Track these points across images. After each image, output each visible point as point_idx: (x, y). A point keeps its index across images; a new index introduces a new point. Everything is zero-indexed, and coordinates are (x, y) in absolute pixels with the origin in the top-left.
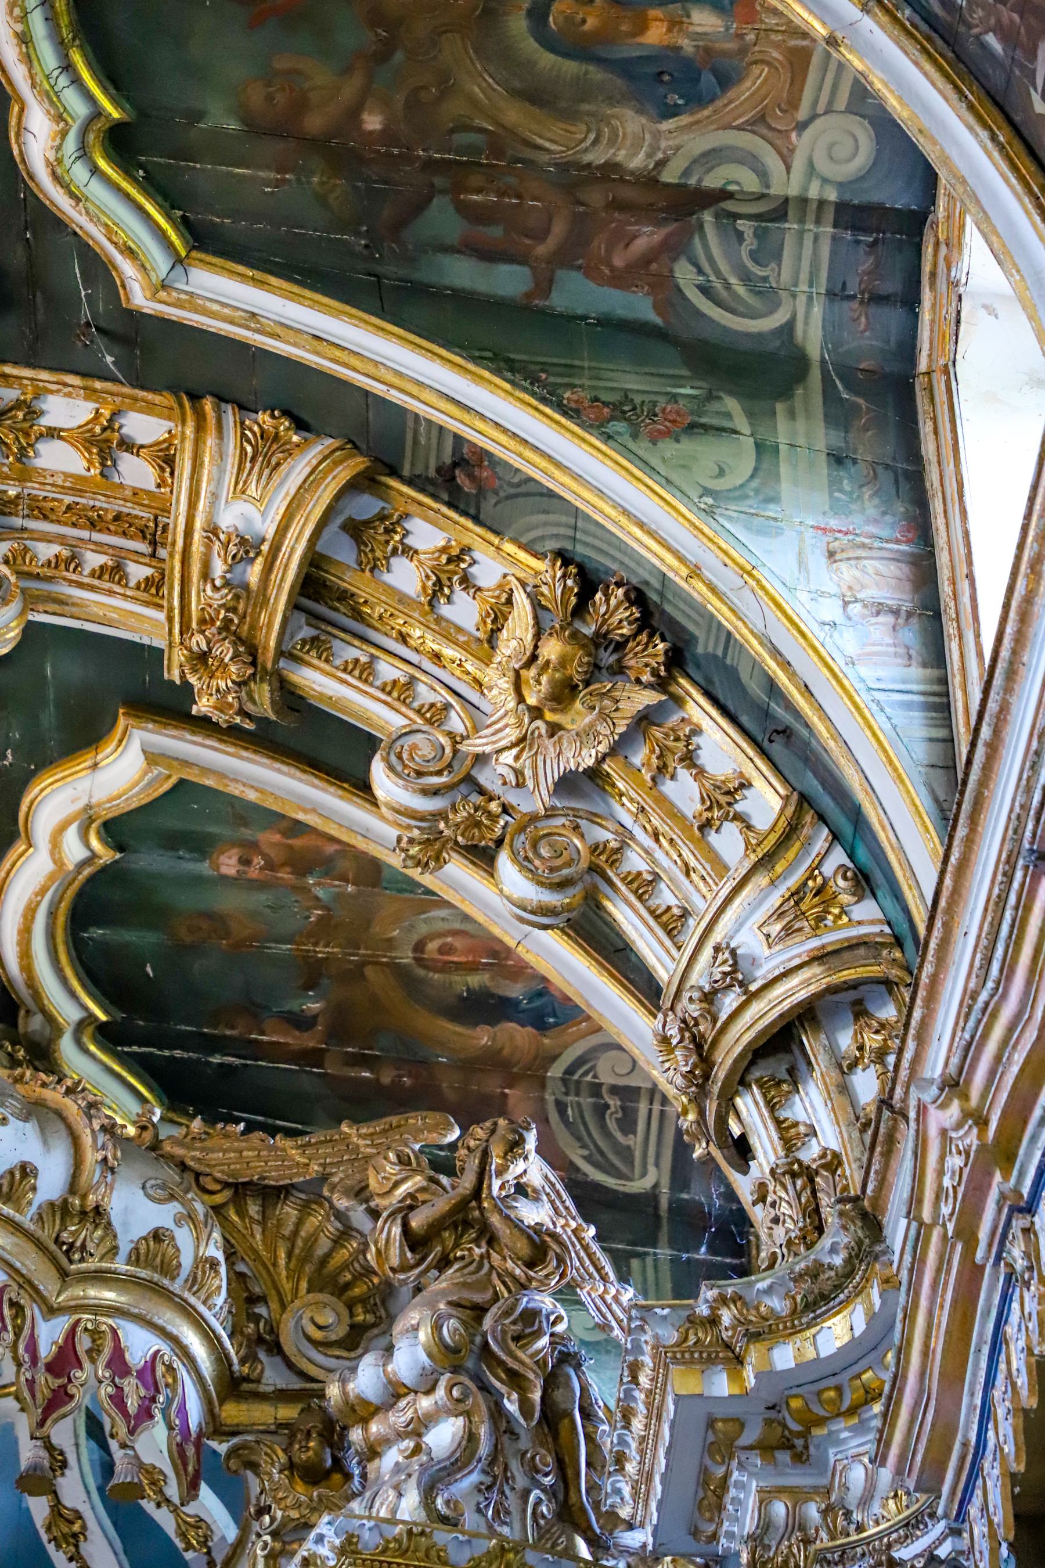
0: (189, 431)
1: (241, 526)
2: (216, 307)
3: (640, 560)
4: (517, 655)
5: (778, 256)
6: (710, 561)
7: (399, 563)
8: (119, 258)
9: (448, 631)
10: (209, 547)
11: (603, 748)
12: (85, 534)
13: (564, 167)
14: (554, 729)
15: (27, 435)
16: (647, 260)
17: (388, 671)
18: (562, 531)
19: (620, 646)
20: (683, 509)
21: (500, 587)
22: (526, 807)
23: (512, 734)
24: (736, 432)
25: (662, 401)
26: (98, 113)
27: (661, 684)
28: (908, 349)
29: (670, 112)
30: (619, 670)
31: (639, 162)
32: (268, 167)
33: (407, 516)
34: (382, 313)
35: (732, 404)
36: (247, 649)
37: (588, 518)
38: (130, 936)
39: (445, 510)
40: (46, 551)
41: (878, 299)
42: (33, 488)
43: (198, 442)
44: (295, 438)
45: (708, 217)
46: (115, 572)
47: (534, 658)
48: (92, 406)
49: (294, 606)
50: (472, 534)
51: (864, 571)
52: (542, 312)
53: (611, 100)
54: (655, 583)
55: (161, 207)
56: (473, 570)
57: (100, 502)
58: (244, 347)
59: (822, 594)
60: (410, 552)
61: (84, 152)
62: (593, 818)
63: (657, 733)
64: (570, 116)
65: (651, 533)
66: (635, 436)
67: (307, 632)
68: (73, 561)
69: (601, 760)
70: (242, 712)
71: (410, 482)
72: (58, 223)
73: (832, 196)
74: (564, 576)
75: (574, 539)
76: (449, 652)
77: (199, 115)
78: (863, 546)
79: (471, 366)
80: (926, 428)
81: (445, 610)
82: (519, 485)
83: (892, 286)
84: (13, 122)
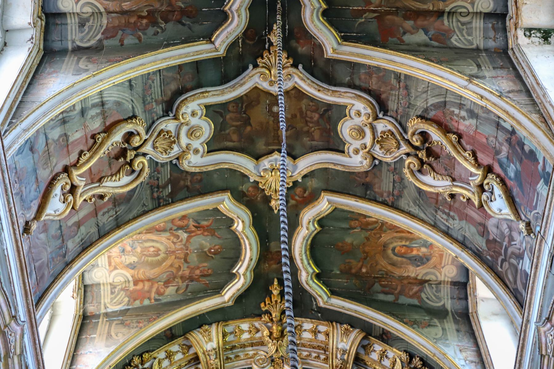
0: (331, 329)
1: (342, 347)
2: (336, 306)
6: (437, 352)
8: (318, 297)
12: (312, 350)
15: (301, 331)
18: (405, 346)
20: (430, 342)
24: (437, 326)
26: (314, 271)
32: (345, 279)
39: (381, 342)
40: (305, 353)
42: (302, 341)
44: (351, 329)
46: (318, 357)
48: (312, 325)
51: (467, 354)
55: (325, 288)
56: (388, 354)
57: (315, 343)
58: (340, 313)
59: (461, 359)
61: (312, 279)
65: (425, 347)
68: (310, 355)
74: (406, 355)
75: (407, 348)
77: (332, 271)
78: (466, 349)
79: (386, 315)
82: (396, 337)
84: (299, 274)
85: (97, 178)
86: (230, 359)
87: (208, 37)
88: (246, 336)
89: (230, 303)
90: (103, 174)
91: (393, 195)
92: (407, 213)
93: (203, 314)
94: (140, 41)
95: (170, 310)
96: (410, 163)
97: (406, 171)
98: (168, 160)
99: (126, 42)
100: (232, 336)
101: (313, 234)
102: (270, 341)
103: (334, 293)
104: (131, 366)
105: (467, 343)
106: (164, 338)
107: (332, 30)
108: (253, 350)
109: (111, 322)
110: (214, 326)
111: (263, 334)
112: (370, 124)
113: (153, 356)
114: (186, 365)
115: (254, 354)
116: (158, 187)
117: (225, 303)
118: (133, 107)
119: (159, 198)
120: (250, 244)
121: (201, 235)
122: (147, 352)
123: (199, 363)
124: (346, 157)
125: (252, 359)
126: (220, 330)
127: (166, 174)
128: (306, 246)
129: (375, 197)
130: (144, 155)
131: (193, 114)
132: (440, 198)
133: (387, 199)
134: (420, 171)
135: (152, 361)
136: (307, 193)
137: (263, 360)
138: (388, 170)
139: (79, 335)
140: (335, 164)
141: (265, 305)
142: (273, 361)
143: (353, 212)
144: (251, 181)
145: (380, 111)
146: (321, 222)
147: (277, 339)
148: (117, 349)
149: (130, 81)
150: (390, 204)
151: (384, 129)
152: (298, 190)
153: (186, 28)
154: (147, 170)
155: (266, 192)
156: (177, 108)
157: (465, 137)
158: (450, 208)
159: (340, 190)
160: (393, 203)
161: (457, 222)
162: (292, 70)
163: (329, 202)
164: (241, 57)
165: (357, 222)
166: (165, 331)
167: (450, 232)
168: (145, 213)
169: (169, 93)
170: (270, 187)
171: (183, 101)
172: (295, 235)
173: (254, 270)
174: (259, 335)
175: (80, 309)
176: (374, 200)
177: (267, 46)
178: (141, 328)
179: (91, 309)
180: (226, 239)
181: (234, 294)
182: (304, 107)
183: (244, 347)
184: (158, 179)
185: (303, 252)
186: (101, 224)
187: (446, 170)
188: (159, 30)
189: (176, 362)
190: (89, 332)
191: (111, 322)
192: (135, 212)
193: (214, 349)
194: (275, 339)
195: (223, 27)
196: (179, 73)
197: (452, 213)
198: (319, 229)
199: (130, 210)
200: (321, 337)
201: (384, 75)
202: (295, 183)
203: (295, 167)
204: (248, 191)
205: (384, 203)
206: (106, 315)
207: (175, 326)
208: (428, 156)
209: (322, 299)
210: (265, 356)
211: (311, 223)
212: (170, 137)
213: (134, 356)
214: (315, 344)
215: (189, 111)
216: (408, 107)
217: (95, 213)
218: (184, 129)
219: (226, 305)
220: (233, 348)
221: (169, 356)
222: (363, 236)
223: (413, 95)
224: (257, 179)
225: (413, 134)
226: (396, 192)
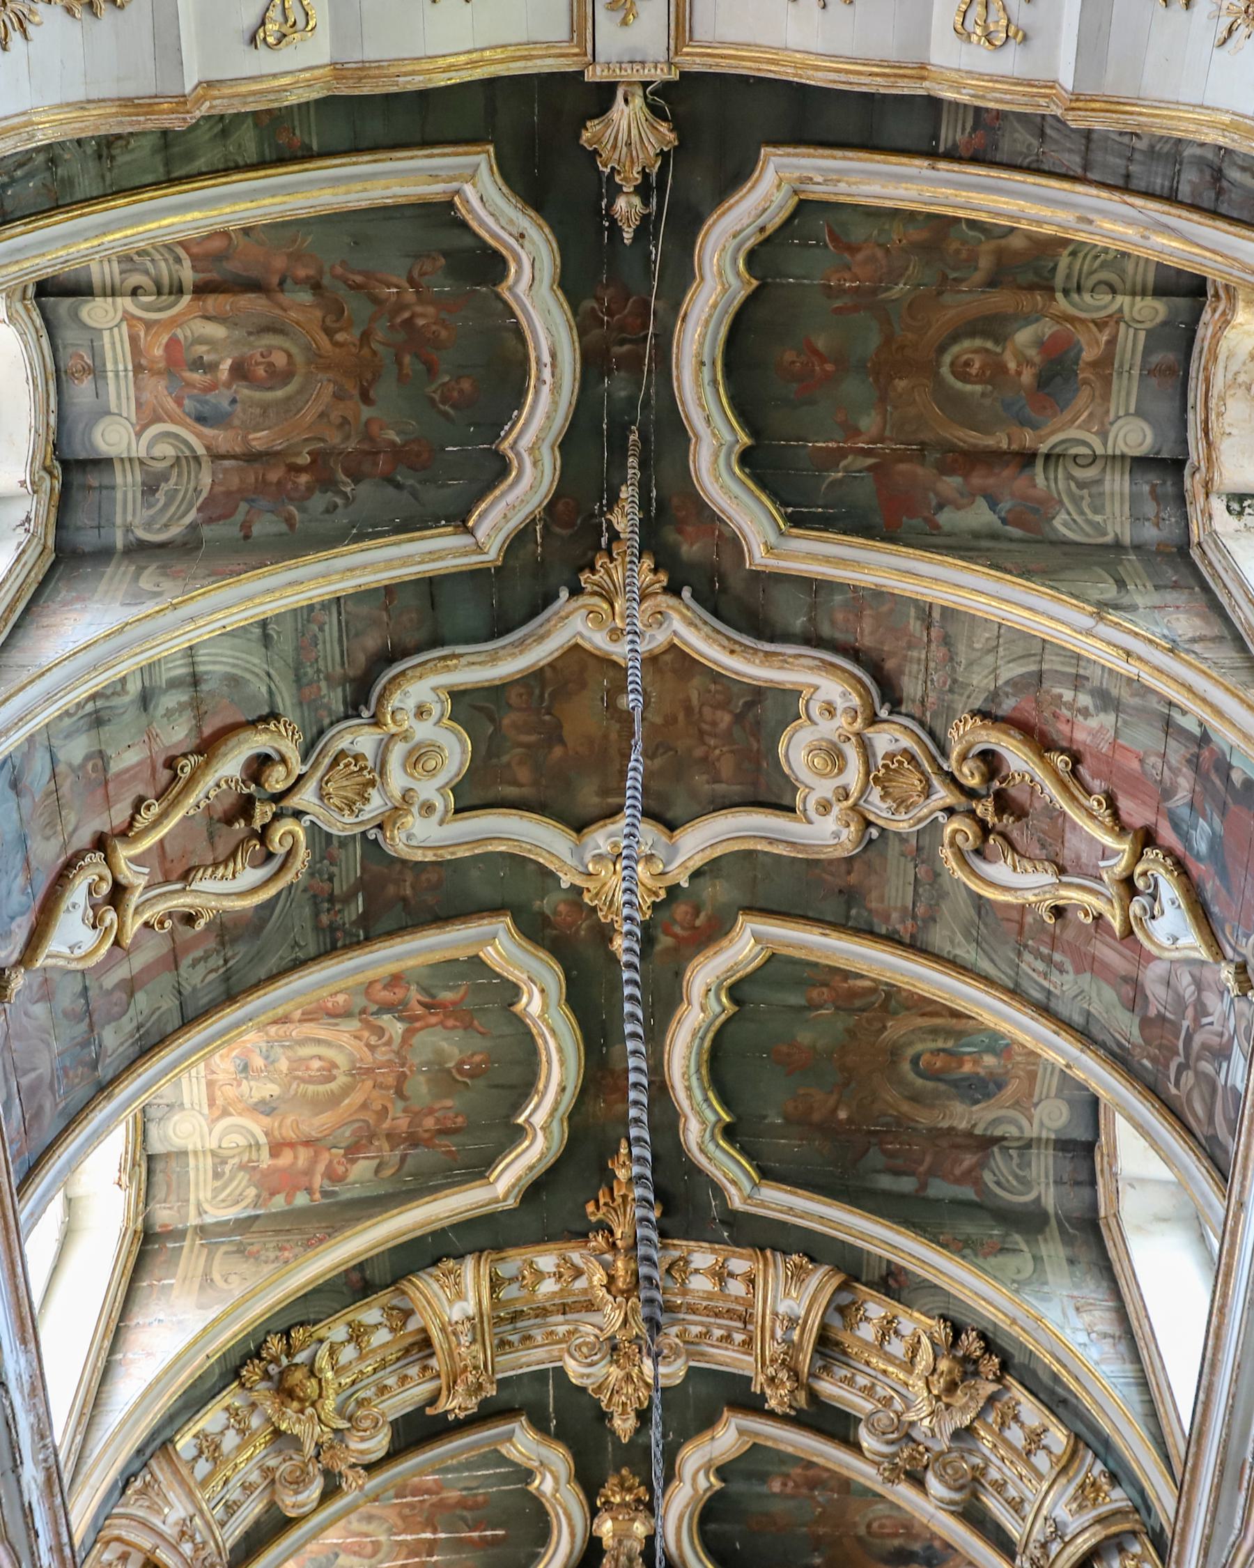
3: (983, 1317)
4: (926, 1368)
5: (1029, 1165)
7: (863, 1325)
8: (728, 1185)
9: (890, 1359)
10: (773, 1321)
11: (973, 1415)
13: (930, 1130)
14: (948, 1406)
16: (970, 1170)
17: (862, 1381)
19: (976, 1362)
21: (913, 1335)
22: (937, 1448)
23: (927, 1410)
25: (985, 1239)
26: (720, 1119)
27: (999, 1380)
28: (1094, 1207)
29: (976, 1102)
30: (976, 1374)
31: (963, 1125)
33: (864, 1302)
34: (851, 1203)
35: (1017, 1237)
36: (795, 1374)
37: (955, 1297)
38: (727, 1527)
40: (695, 1330)
41: (1077, 1183)
42: (689, 1299)
43: (765, 1271)
45: (996, 1149)
46: (727, 1338)
47: (934, 1370)
49: (815, 1350)
50: (898, 1308)
52: (927, 1200)
53: (949, 1098)
54: (991, 1328)
58: (784, 1224)
60: (868, 1319)
61: (713, 1137)
62: (970, 1452)
63: (998, 1405)
64: (932, 1107)
66: (976, 1255)
67: (820, 1363)
69: (972, 1421)
70: (791, 1407)
71: (866, 1285)
72: (695, 1170)
73: (1053, 1136)
76: (891, 1369)
77: (765, 1117)
80: (1109, 1244)
81: (887, 1347)
83: (1083, 1176)
86: (510, 1344)
88: (548, 1287)
89: (511, 1203)
92: (949, 961)
93: (443, 1229)
95: (358, 1220)
100: (515, 1286)
101: (718, 1023)
102: (610, 1298)
103: (766, 1174)
104: (261, 1359)
106: (345, 1289)
108: (567, 1322)
109: (211, 1248)
110: (470, 1262)
111: (590, 1281)
113: (315, 1336)
114: (398, 1359)
115: (569, 1332)
117: (496, 1201)
120: (560, 1050)
121: (439, 1028)
122: (302, 1324)
124: (799, 821)
125: (564, 1346)
126: (485, 1270)
128: (699, 1054)
129: (870, 924)
133: (899, 927)
135: (313, 1347)
136: (703, 916)
137: (591, 1346)
140: (771, 841)
141: (598, 1208)
142: (614, 1348)
143: (816, 965)
144: (564, 885)
146: (737, 992)
147: (627, 1294)
148: (226, 1314)
150: (907, 940)
152: (681, 910)
155: (600, 914)
159: (783, 909)
163: (758, 938)
165: (825, 990)
166: (346, 1271)
170: (612, 901)
172: (673, 1025)
173: (570, 1117)
174: (581, 1284)
175: (137, 1215)
176: (867, 932)
178: (286, 1262)
179: (164, 1215)
180: (501, 1036)
181: (519, 1179)
183: (545, 1316)
185: (693, 1069)
189: (373, 1351)
190: (158, 1272)
191: (211, 1248)
193: (469, 1319)
194: (622, 1292)
198: (731, 1009)
200: (737, 1288)
202: (673, 890)
203: (673, 850)
205: (892, 939)
206: (202, 1230)
207: (371, 1258)
209: (740, 1189)
210: (597, 1337)
211: (712, 994)
213: (268, 1333)
214: (722, 1305)
219: (500, 1207)
220: (516, 1316)
221: (357, 1334)
222: (840, 1026)
224: (580, 881)
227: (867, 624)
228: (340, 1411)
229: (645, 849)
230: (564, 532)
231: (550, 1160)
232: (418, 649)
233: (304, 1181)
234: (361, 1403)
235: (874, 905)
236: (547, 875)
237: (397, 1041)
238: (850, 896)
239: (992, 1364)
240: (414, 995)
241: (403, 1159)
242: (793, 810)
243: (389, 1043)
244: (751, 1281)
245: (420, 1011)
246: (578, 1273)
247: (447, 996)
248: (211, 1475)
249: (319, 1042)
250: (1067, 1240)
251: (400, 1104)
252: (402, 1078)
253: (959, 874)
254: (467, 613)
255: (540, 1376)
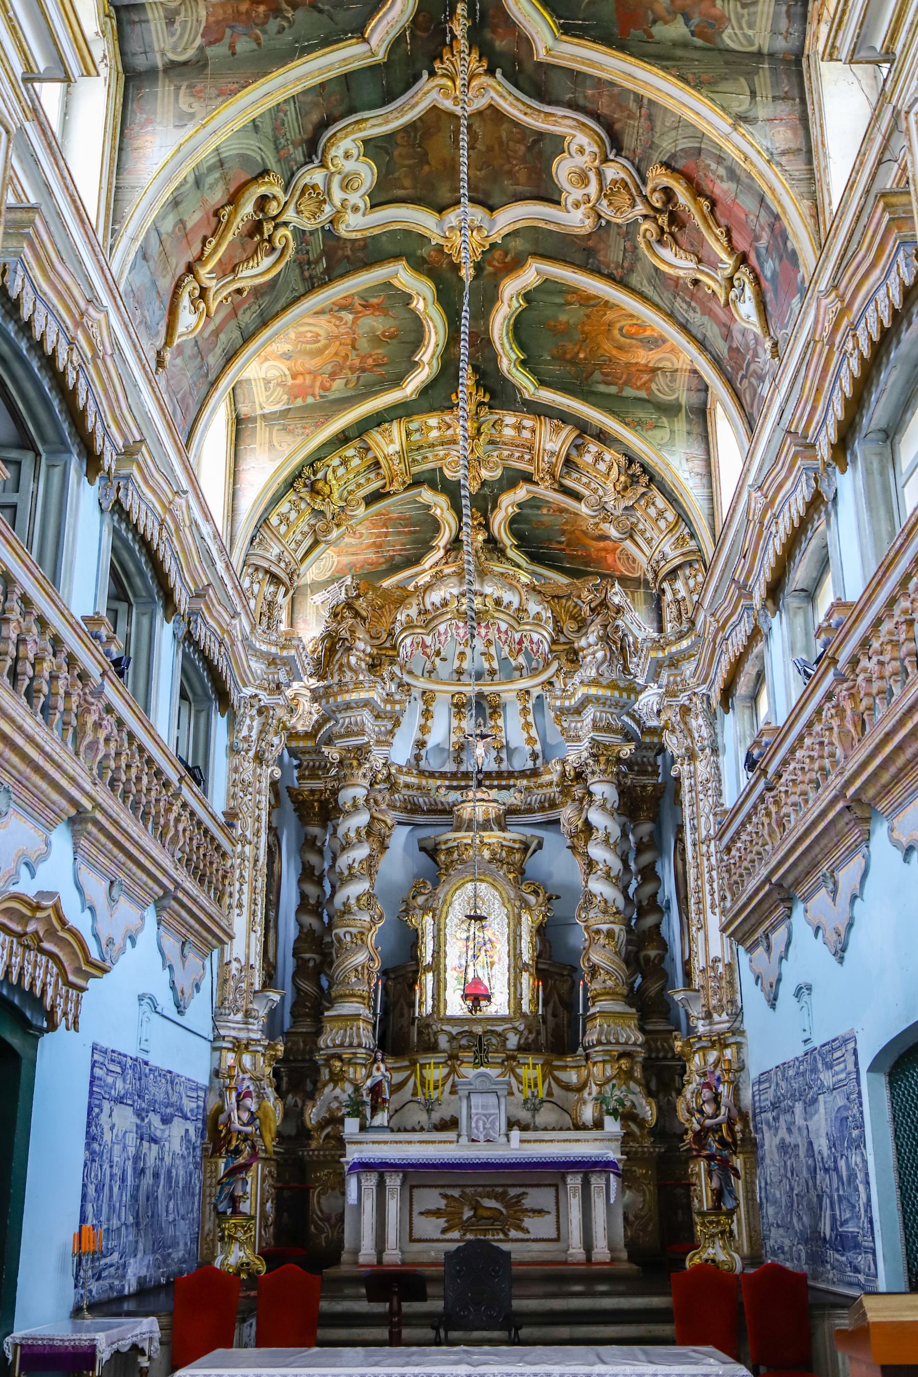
16: (645, 384)
28: (705, 403)
35: (664, 419)
40: (506, 453)
41: (699, 390)
68: (512, 455)
72: (505, 380)
85: (230, 268)
87: (359, 32)
88: (434, 434)
89: (414, 397)
90: (237, 261)
91: (623, 268)
94: (259, 44)
96: (647, 230)
97: (640, 239)
98: (319, 226)
99: (239, 48)
105: (697, 450)
107: (546, 15)
112: (597, 168)
116: (309, 263)
118: (262, 159)
119: (311, 277)
120: (435, 327)
123: (380, 467)
127: (318, 244)
130: (286, 224)
131: (347, 156)
132: (681, 281)
134: (660, 241)
136: (509, 257)
138: (618, 234)
139: (236, 446)
140: (547, 222)
144: (433, 243)
145: (612, 149)
149: (254, 120)
151: (616, 177)
152: (497, 254)
153: (325, 17)
154: (292, 244)
156: (324, 151)
157: (719, 206)
158: (692, 296)
160: (621, 278)
161: (699, 315)
162: (486, 80)
164: (410, 60)
167: (689, 326)
168: (296, 300)
169: (310, 127)
171: (330, 138)
172: (494, 312)
174: (450, 432)
177: (448, 39)
182: (504, 135)
184: (307, 253)
186: (243, 326)
187: (692, 245)
188: (285, 24)
192: (282, 302)
195: (381, 14)
196: (321, 95)
197: (693, 304)
199: (276, 300)
200: (526, 434)
201: (620, 94)
204: (429, 256)
208: (671, 223)
212: (318, 194)
215: (340, 153)
216: (650, 148)
217: (234, 312)
218: (336, 180)
220: (420, 448)
223: (658, 129)
225: (654, 190)
226: (626, 264)
227: (604, 100)
228: (340, 498)
229: (477, 223)
230: (424, 35)
231: (432, 376)
232: (342, 116)
233: (310, 390)
234: (349, 493)
235: (602, 258)
236: (423, 239)
237: (350, 323)
238: (590, 252)
239: (645, 479)
240: (357, 301)
241: (358, 378)
242: (558, 203)
243: (346, 324)
244: (534, 431)
245: (360, 308)
246: (449, 427)
247: (374, 301)
248: (287, 531)
249: (310, 324)
250: (689, 421)
251: (354, 353)
252: (354, 340)
253: (646, 252)
254: (369, 91)
255: (434, 470)
